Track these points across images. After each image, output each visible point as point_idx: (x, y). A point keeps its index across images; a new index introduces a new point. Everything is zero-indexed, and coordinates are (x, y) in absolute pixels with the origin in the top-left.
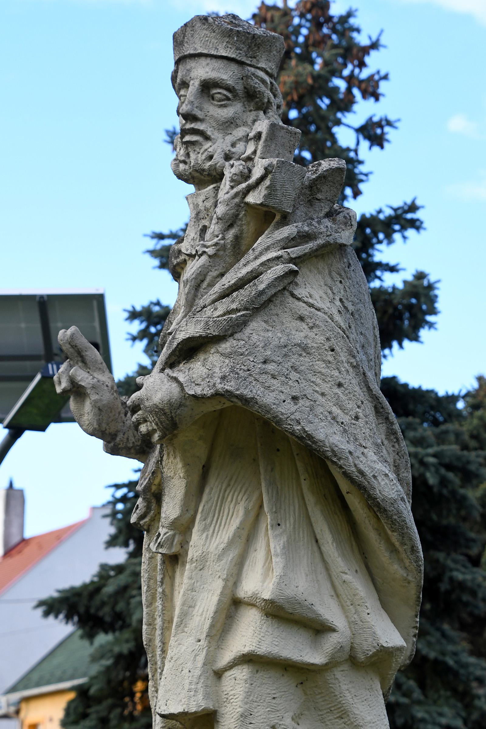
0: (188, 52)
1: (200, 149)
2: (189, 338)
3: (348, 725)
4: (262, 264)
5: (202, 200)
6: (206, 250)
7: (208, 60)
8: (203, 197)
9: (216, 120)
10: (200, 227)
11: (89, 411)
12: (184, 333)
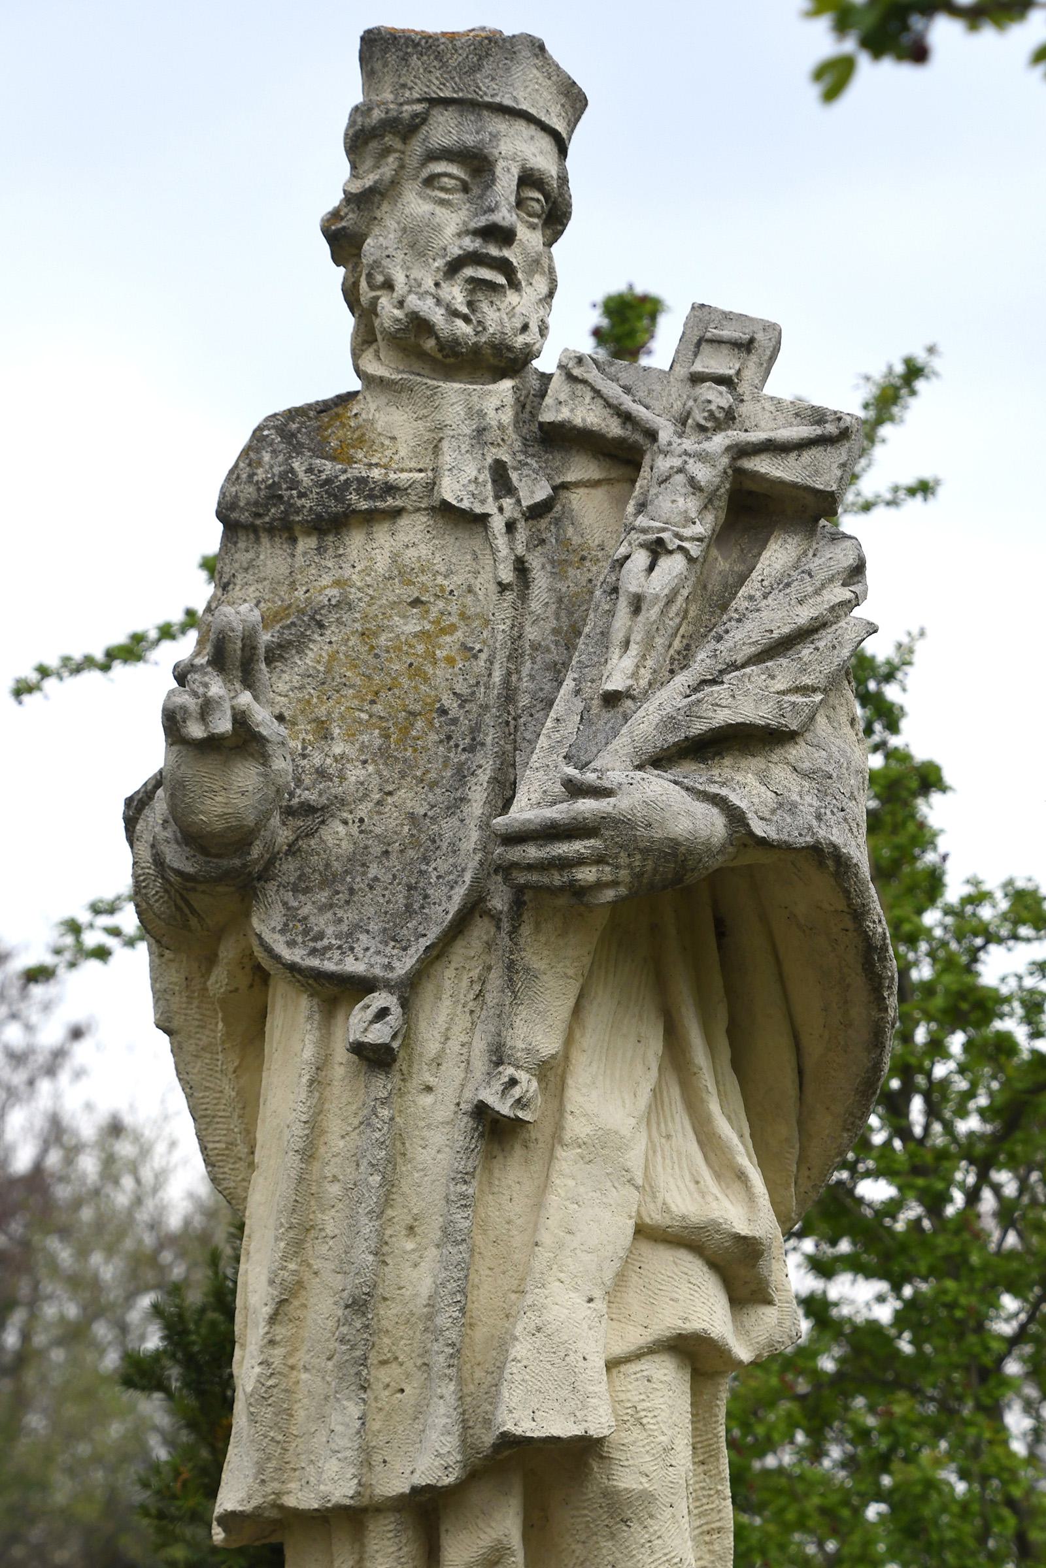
0: (498, 99)
1: (502, 302)
2: (742, 724)
3: (710, 1476)
4: (832, 609)
5: (493, 406)
6: (683, 544)
7: (533, 130)
8: (494, 402)
9: (525, 252)
10: (489, 460)
11: (250, 788)
12: (727, 711)
